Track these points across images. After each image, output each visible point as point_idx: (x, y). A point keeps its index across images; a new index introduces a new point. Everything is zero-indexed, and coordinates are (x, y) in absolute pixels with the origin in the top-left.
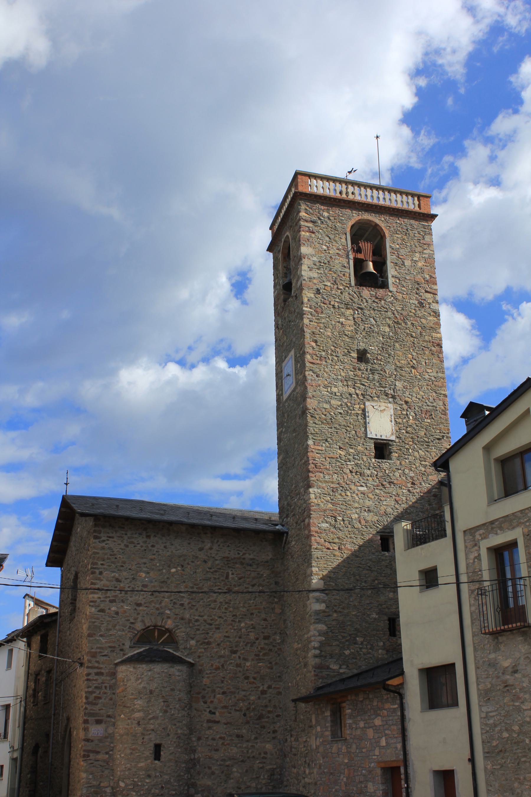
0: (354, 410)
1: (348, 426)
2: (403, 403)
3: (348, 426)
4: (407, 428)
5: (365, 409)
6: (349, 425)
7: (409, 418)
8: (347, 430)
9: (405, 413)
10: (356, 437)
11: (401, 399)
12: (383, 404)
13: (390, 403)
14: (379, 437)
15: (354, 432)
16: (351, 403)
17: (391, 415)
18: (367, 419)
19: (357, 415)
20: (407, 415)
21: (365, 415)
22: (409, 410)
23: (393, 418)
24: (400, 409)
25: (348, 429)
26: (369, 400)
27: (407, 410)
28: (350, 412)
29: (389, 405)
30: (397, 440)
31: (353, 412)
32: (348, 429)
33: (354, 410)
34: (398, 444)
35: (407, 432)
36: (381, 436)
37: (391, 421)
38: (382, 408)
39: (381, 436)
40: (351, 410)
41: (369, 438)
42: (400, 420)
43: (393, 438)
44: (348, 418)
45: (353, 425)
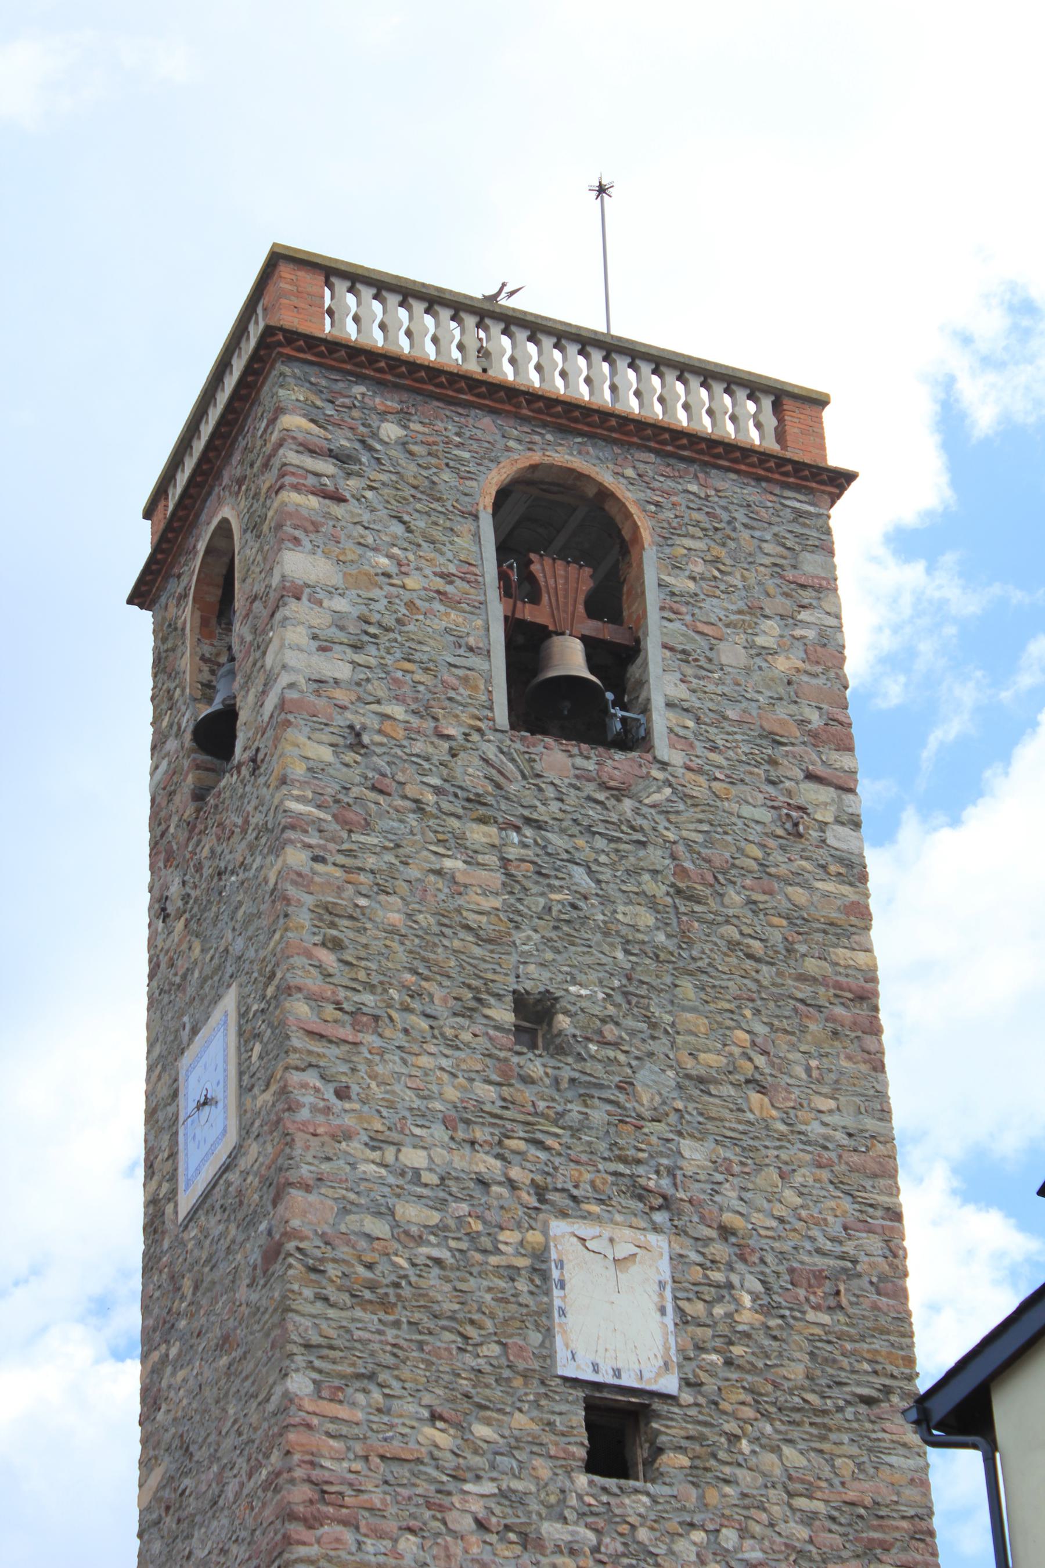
0: (498, 1251)
1: (472, 1322)
2: (713, 1234)
3: (472, 1322)
4: (731, 1343)
5: (546, 1248)
6: (476, 1317)
7: (736, 1301)
8: (466, 1338)
9: (718, 1276)
10: (506, 1373)
11: (702, 1218)
12: (628, 1232)
13: (656, 1229)
14: (606, 1377)
15: (496, 1349)
16: (485, 1222)
17: (662, 1285)
18: (556, 1292)
19: (512, 1273)
20: (730, 1286)
21: (545, 1276)
22: (739, 1266)
23: (668, 1294)
24: (699, 1259)
25: (471, 1331)
26: (563, 1214)
27: (732, 1269)
28: (478, 1257)
29: (653, 1238)
30: (687, 1398)
31: (493, 1260)
32: (471, 1331)
33: (498, 1251)
34: (693, 1412)
35: (729, 1363)
36: (617, 1373)
37: (662, 1311)
38: (624, 1250)
39: (617, 1373)
40: (485, 1251)
41: (566, 1379)
42: (696, 1309)
43: (670, 1384)
44: (473, 1283)
45: (492, 1316)
